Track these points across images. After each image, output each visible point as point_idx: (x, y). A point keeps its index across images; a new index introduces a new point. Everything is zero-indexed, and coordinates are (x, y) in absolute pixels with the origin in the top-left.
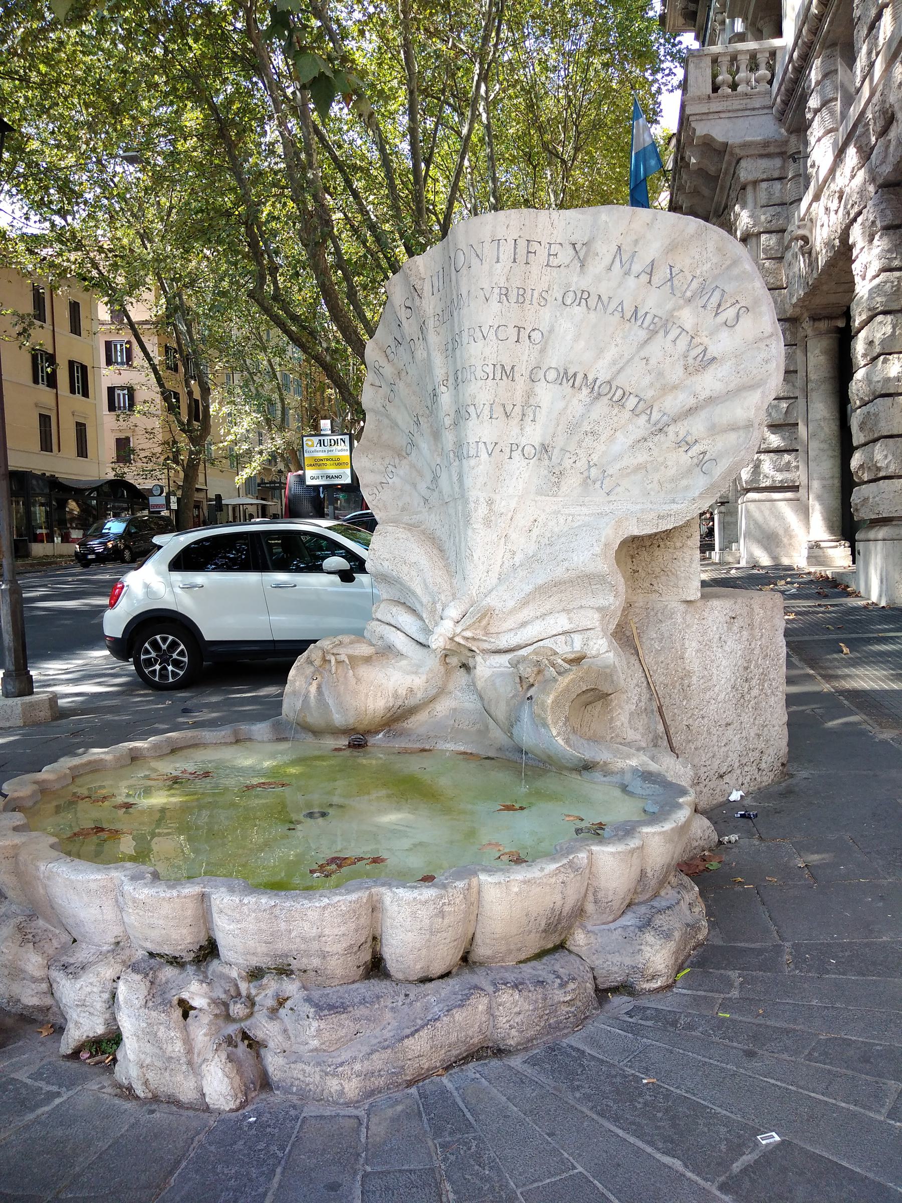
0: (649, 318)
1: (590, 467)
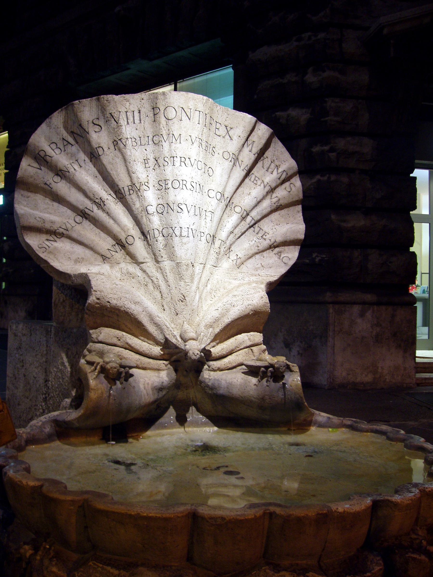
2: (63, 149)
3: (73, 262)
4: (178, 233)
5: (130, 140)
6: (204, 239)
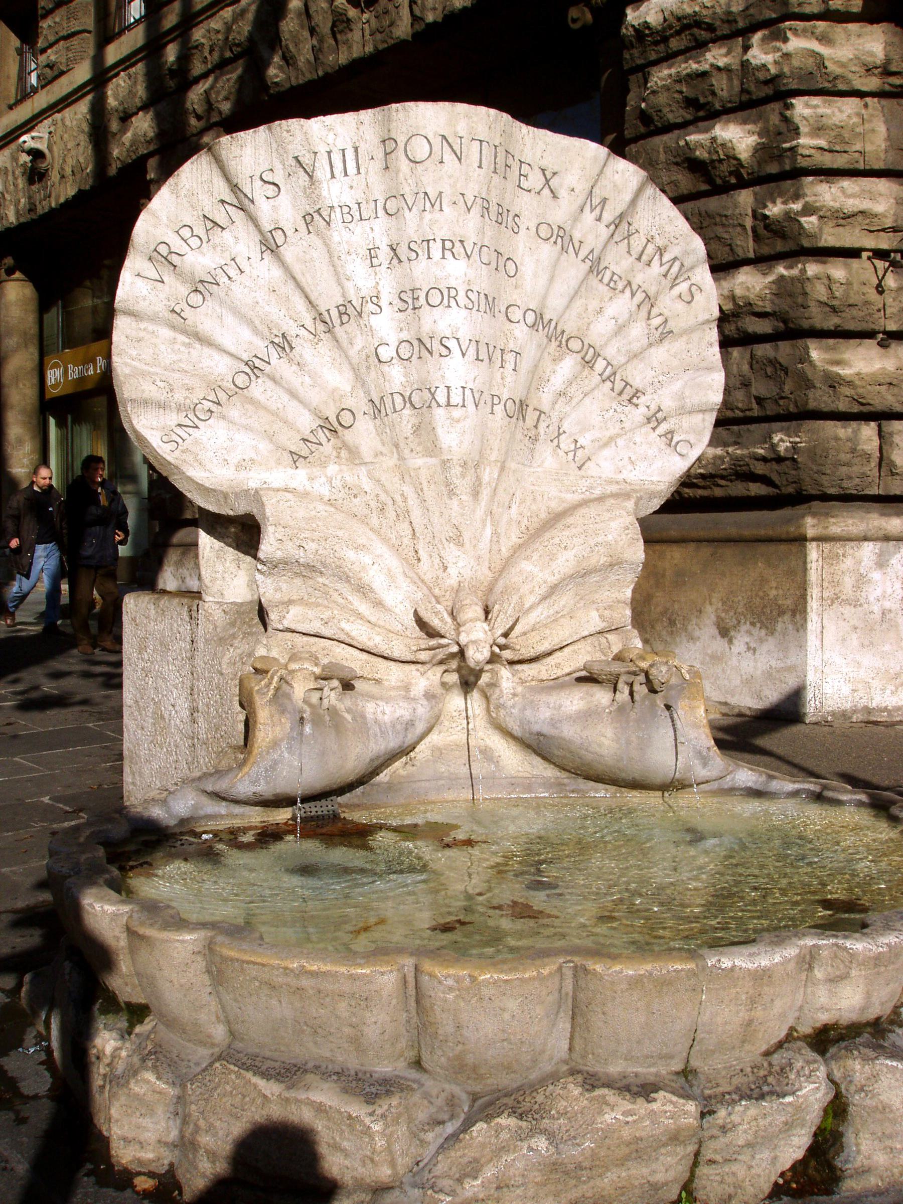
0: (608, 274)
1: (559, 434)
2: (204, 238)
3: (233, 468)
4: (441, 397)
5: (338, 210)
6: (498, 409)
